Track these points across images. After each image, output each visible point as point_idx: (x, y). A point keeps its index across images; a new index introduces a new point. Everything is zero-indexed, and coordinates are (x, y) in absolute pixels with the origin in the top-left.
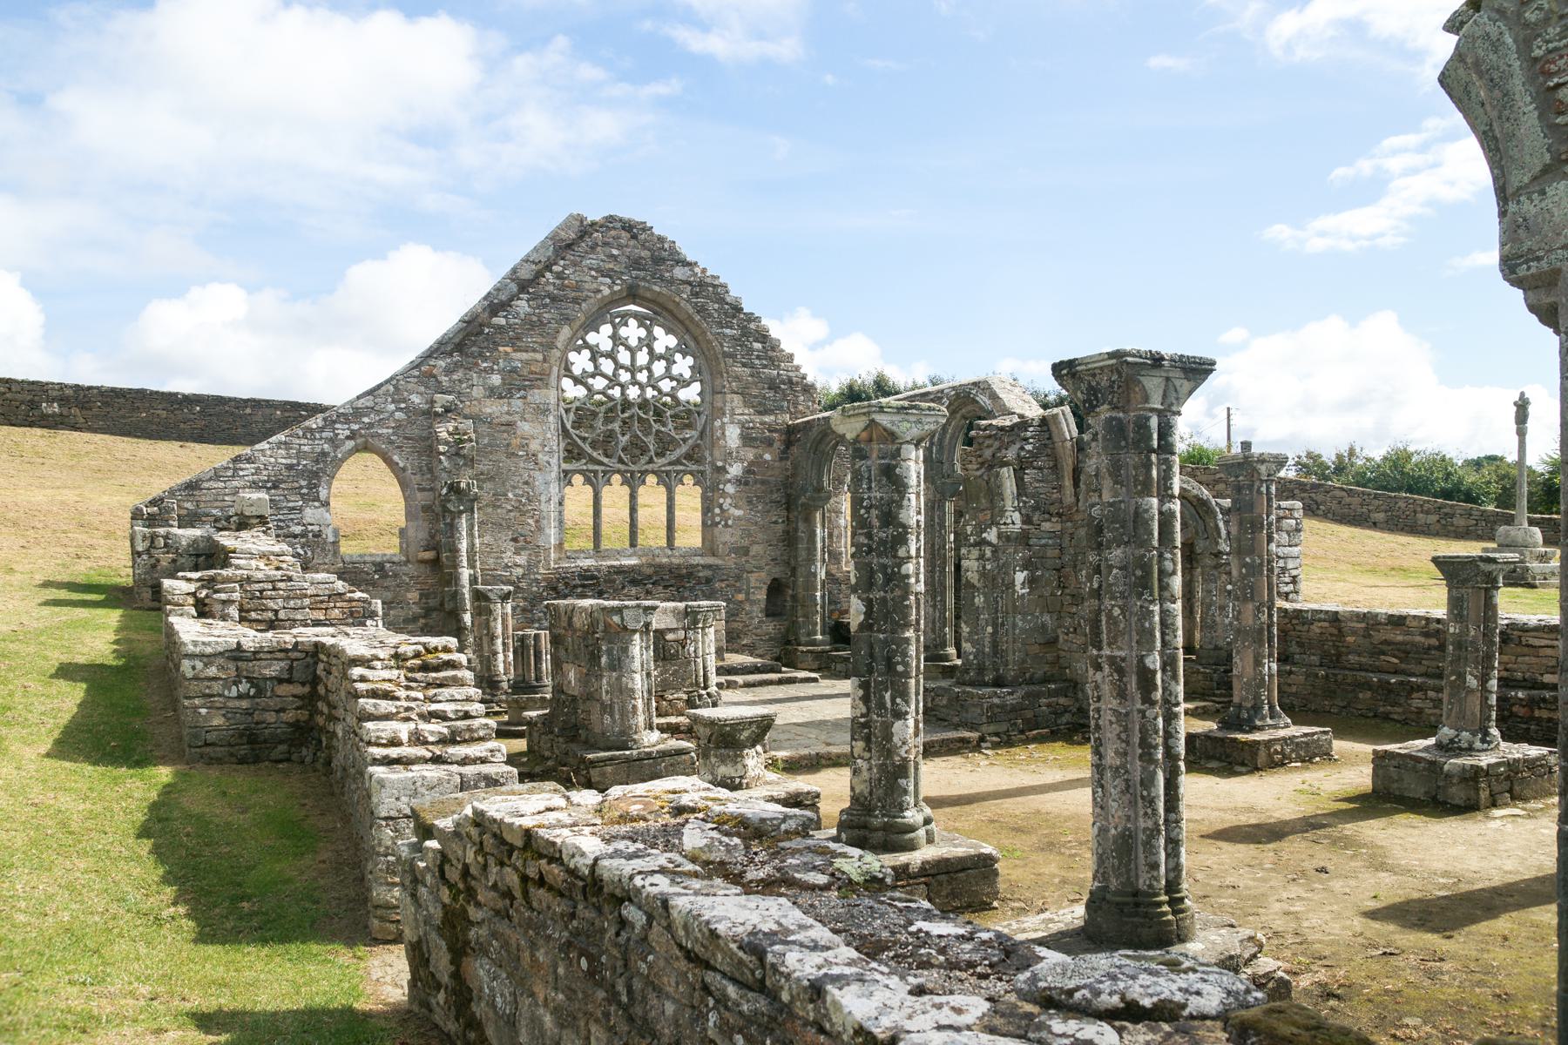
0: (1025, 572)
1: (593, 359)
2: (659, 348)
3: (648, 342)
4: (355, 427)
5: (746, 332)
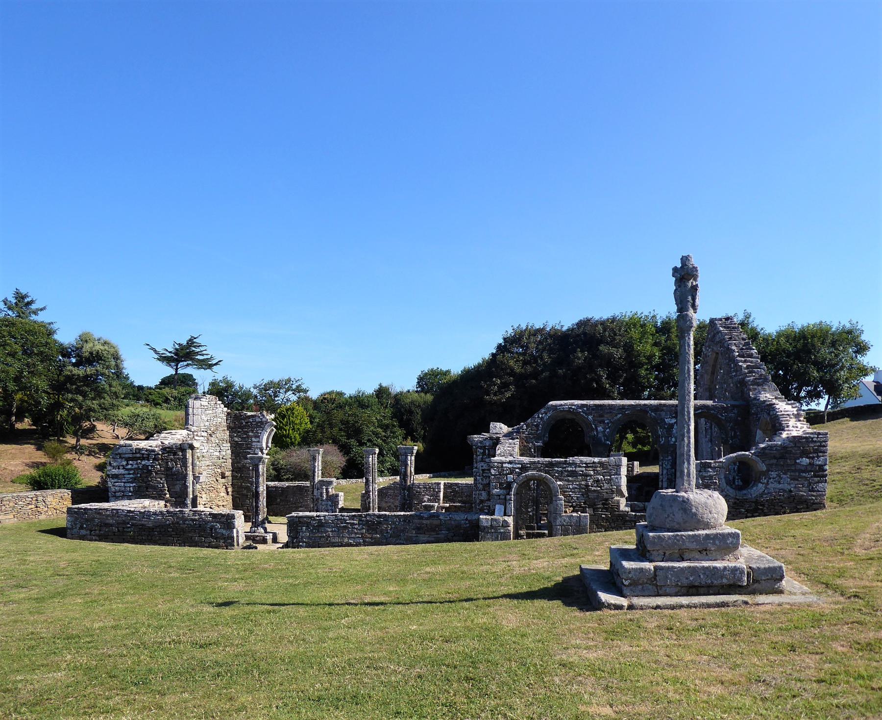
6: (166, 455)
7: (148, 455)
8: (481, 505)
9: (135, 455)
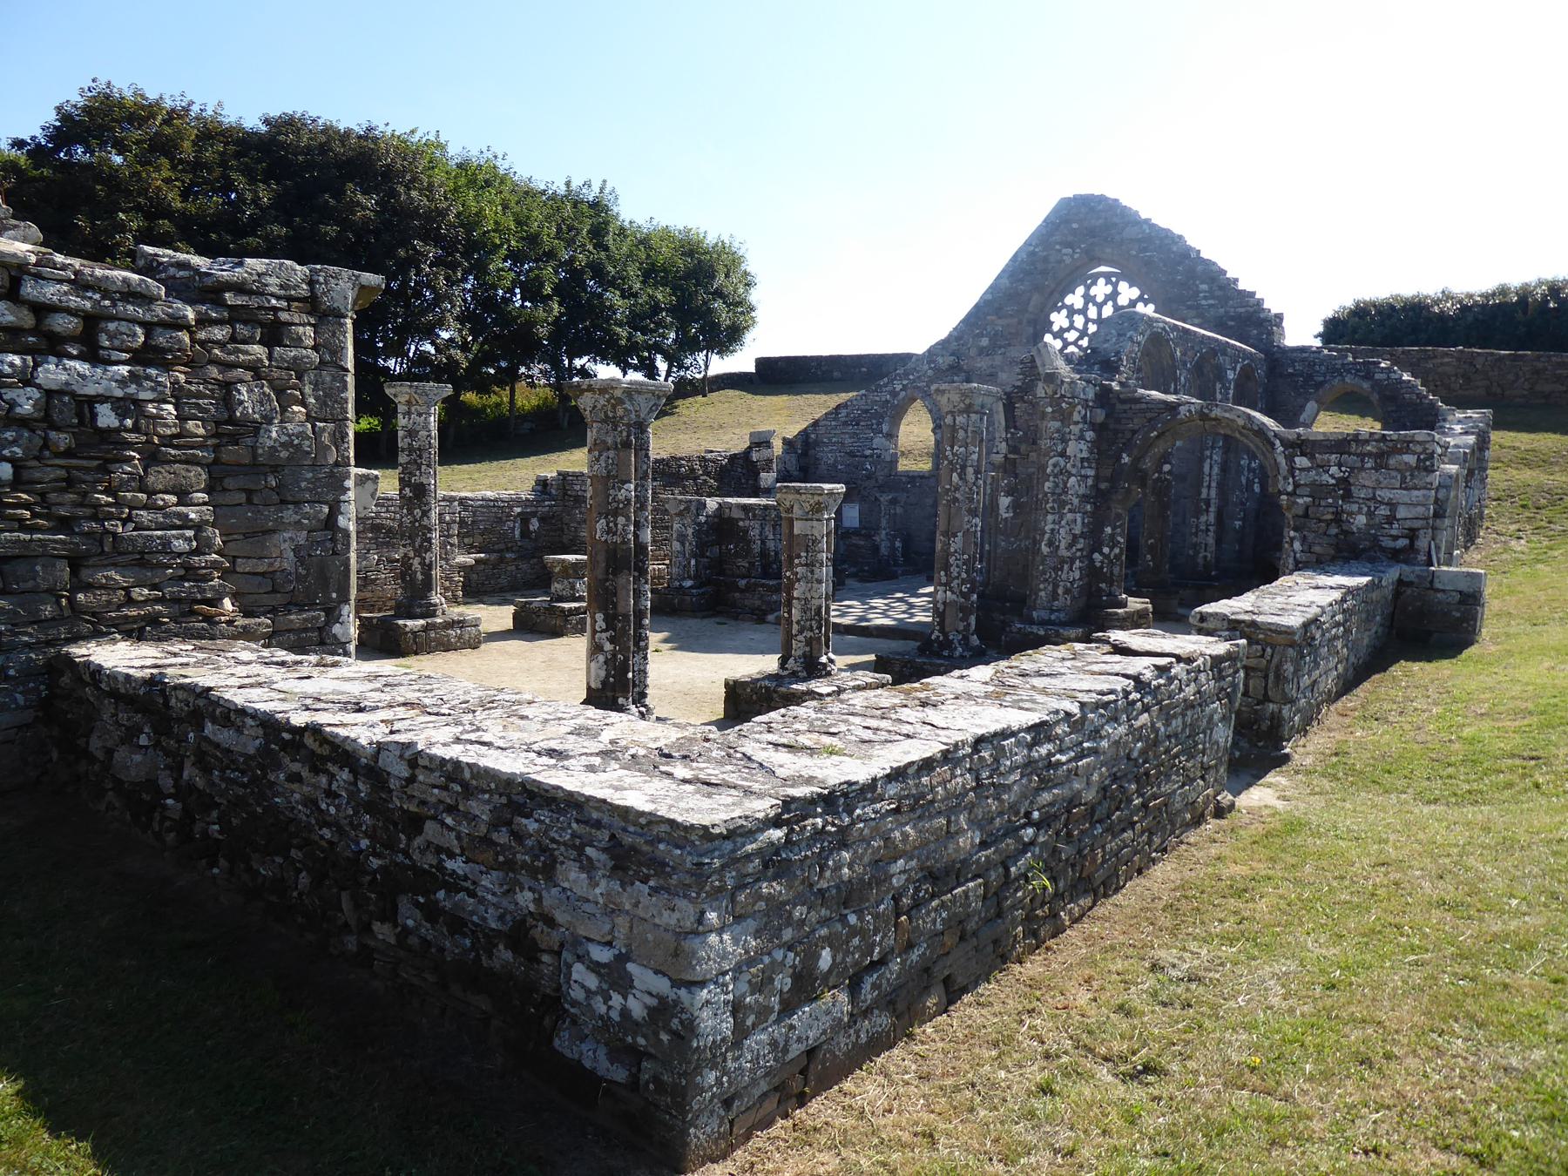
0: (1010, 498)
1: (1070, 317)
4: (905, 382)
6: (219, 333)
7: (92, 322)
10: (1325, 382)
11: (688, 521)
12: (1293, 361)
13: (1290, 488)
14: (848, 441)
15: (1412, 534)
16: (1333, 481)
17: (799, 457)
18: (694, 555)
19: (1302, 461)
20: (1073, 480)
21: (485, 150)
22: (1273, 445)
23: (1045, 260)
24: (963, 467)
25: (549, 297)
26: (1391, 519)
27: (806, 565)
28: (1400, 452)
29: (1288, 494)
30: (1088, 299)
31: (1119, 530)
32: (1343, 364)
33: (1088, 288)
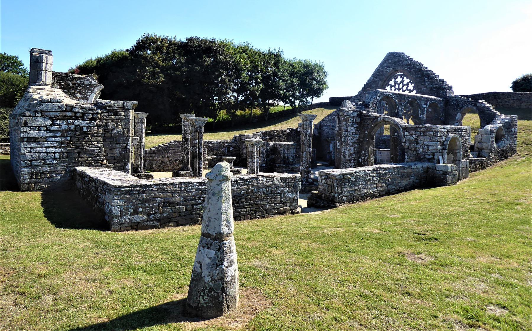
2: (405, 83)
3: (402, 81)
5: (422, 75)
6: (105, 114)
7: (83, 114)
8: (351, 157)
9: (64, 114)
10: (462, 107)
11: (264, 148)
12: (453, 101)
13: (404, 141)
14: (332, 125)
15: (433, 154)
16: (414, 139)
17: (318, 130)
18: (266, 158)
19: (407, 133)
20: (349, 138)
21: (246, 42)
22: (400, 129)
23: (382, 71)
24: (306, 135)
25: (260, 83)
26: (428, 150)
27: (251, 159)
28: (429, 131)
29: (404, 142)
30: (396, 83)
31: (367, 152)
32: (468, 102)
33: (395, 79)
